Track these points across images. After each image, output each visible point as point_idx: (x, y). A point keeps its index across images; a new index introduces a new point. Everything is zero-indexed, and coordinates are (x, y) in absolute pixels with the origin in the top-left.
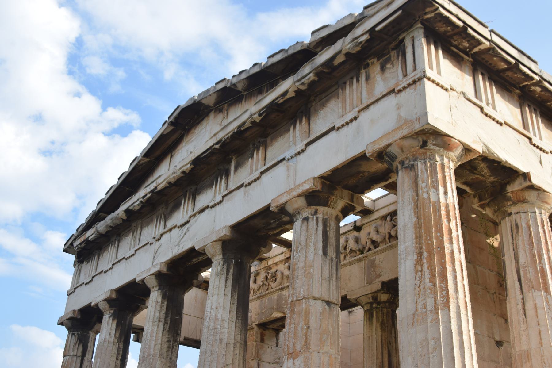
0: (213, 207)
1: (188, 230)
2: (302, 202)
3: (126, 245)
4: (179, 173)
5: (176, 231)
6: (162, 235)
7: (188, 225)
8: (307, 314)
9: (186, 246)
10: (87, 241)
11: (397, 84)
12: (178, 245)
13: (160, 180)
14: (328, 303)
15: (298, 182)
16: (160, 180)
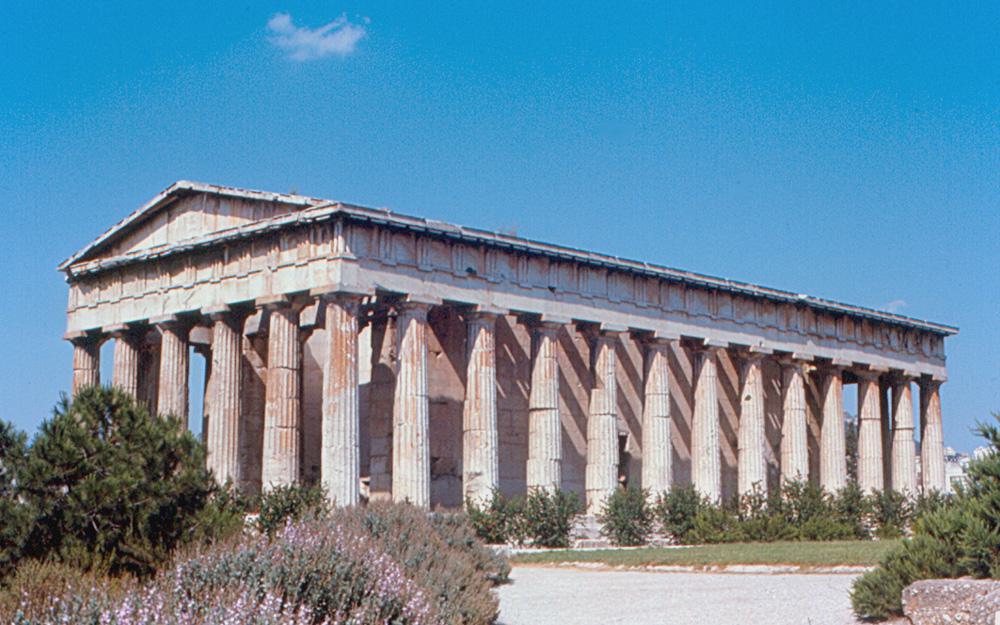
0: (213, 283)
1: (192, 295)
2: (275, 307)
3: (132, 286)
4: (182, 249)
5: (181, 291)
6: (169, 289)
7: (191, 291)
8: (278, 376)
9: (194, 307)
10: (88, 271)
11: (329, 255)
12: (186, 303)
13: (166, 248)
14: (293, 369)
15: (275, 292)
16: (166, 248)
